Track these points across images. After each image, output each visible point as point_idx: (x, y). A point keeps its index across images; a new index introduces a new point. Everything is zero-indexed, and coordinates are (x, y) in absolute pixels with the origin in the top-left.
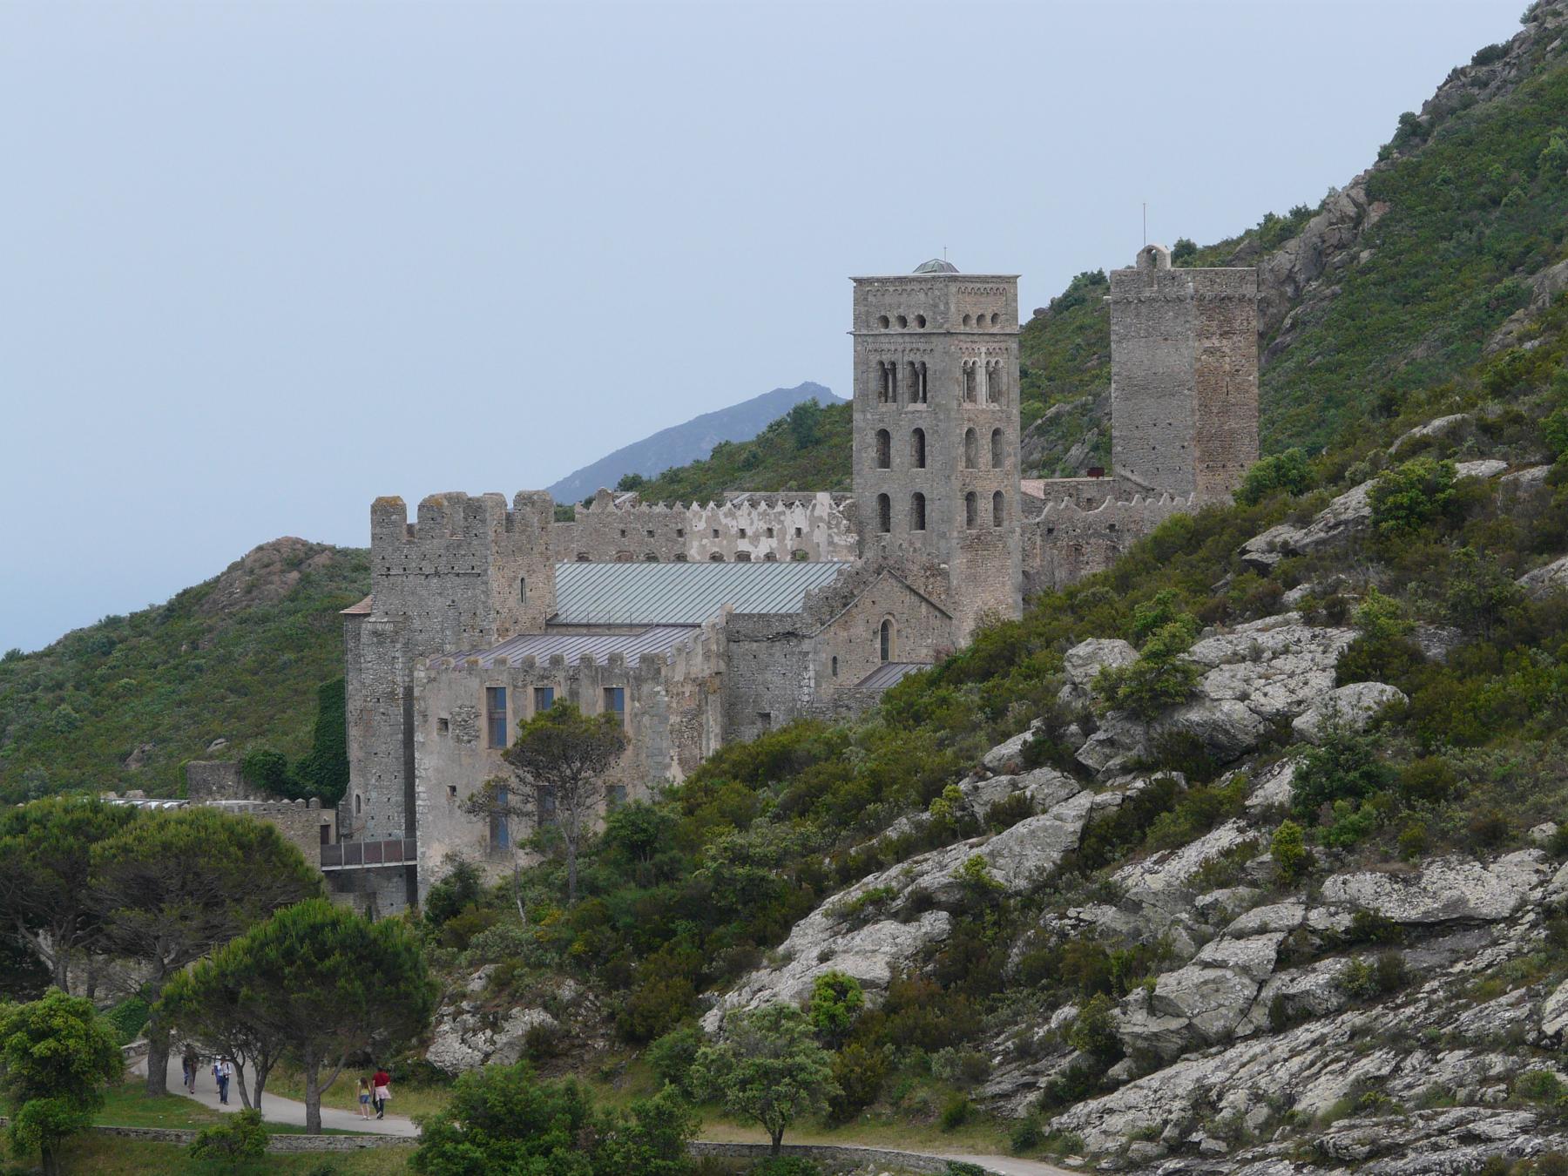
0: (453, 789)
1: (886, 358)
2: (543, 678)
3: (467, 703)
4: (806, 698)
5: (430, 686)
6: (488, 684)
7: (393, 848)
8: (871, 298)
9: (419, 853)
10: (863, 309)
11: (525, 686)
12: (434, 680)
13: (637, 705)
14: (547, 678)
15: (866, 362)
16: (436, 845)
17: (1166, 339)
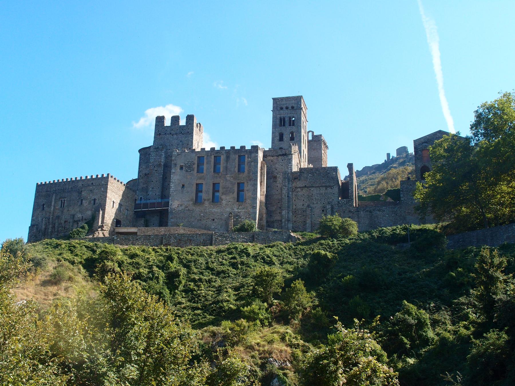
0: (183, 186)
1: (282, 116)
2: (217, 153)
3: (191, 161)
4: (290, 171)
5: (178, 156)
6: (198, 155)
7: (159, 204)
8: (278, 103)
9: (170, 204)
10: (275, 105)
11: (211, 155)
12: (180, 155)
13: (250, 159)
14: (219, 153)
15: (276, 117)
16: (176, 201)
17: (314, 150)
